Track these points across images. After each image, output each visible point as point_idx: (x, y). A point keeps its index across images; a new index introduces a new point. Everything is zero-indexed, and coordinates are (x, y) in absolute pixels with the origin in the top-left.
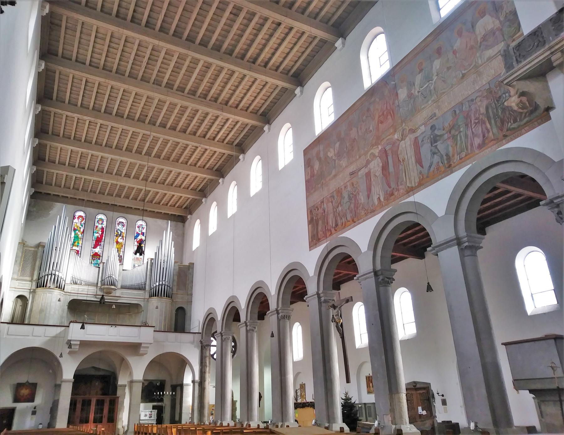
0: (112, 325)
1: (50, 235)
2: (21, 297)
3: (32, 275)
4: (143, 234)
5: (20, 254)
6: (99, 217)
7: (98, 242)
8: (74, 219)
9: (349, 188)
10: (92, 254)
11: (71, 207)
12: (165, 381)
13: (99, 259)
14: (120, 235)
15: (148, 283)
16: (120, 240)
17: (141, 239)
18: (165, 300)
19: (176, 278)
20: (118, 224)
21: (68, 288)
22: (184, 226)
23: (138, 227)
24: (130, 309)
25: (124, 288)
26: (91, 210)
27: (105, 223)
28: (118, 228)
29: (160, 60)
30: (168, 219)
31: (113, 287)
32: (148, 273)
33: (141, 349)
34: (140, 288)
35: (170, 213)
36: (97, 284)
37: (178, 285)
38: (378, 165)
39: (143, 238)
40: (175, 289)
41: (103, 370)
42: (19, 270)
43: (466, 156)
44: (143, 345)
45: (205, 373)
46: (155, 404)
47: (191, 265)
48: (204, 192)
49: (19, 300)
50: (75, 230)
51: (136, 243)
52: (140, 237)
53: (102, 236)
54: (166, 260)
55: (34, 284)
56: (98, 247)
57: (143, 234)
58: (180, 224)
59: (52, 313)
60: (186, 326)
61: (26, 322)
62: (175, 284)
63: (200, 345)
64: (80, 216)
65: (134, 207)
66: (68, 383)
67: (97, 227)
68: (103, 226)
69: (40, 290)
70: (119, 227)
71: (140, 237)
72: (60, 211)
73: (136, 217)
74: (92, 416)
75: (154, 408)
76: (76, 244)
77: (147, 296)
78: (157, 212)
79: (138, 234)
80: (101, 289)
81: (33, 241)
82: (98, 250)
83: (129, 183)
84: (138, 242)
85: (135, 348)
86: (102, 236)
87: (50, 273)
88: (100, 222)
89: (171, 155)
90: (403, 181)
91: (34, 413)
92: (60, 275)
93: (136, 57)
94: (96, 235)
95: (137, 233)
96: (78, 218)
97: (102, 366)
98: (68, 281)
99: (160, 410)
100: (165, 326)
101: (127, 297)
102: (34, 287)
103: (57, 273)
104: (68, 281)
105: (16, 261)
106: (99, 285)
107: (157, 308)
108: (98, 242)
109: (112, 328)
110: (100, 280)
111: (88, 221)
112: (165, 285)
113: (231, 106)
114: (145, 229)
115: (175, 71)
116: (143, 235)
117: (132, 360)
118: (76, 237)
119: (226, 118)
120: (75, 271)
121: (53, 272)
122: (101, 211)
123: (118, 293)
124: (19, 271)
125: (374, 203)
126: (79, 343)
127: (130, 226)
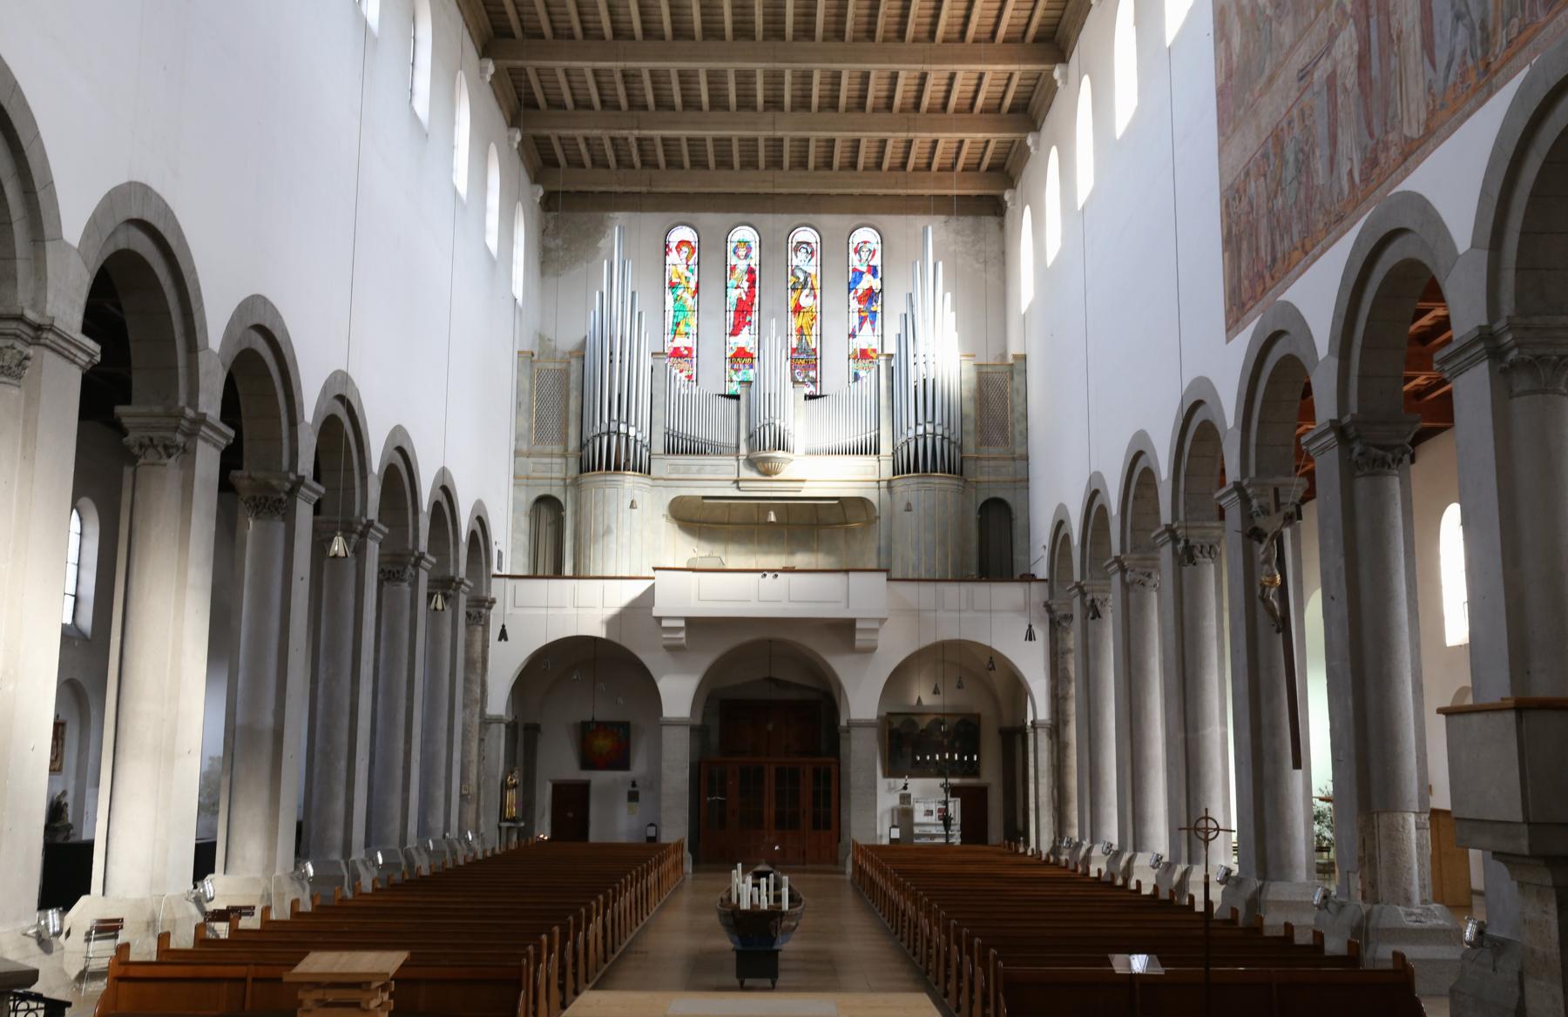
1: (593, 318)
3: (564, 440)
4: (873, 271)
5: (526, 384)
7: (743, 309)
8: (666, 254)
9: (1297, 131)
10: (729, 354)
11: (651, 221)
12: (979, 716)
13: (751, 366)
14: (804, 287)
16: (806, 301)
17: (871, 289)
19: (970, 409)
20: (796, 250)
22: (1002, 226)
23: (857, 251)
26: (710, 219)
27: (755, 253)
33: (858, 636)
36: (738, 447)
38: (1351, 47)
39: (876, 284)
43: (1520, 33)
44: (859, 625)
45: (1065, 698)
46: (954, 781)
48: (1028, 111)
49: (544, 510)
51: (855, 305)
57: (873, 271)
58: (990, 222)
63: (1047, 616)
64: (682, 243)
67: (733, 268)
69: (588, 477)
70: (801, 261)
71: (863, 285)
73: (846, 220)
74: (769, 811)
75: (954, 791)
76: (682, 328)
81: (566, 340)
82: (745, 339)
85: (843, 630)
87: (604, 429)
89: (875, 23)
90: (1395, 116)
91: (633, 797)
92: (632, 432)
94: (734, 295)
95: (855, 270)
96: (678, 247)
97: (794, 677)
99: (974, 802)
102: (573, 470)
104: (658, 447)
105: (519, 405)
106: (743, 450)
107: (909, 508)
110: (743, 436)
111: (709, 252)
112: (934, 435)
114: (878, 254)
121: (613, 427)
122: (739, 217)
125: (1341, 192)
126: (682, 624)
127: (832, 250)
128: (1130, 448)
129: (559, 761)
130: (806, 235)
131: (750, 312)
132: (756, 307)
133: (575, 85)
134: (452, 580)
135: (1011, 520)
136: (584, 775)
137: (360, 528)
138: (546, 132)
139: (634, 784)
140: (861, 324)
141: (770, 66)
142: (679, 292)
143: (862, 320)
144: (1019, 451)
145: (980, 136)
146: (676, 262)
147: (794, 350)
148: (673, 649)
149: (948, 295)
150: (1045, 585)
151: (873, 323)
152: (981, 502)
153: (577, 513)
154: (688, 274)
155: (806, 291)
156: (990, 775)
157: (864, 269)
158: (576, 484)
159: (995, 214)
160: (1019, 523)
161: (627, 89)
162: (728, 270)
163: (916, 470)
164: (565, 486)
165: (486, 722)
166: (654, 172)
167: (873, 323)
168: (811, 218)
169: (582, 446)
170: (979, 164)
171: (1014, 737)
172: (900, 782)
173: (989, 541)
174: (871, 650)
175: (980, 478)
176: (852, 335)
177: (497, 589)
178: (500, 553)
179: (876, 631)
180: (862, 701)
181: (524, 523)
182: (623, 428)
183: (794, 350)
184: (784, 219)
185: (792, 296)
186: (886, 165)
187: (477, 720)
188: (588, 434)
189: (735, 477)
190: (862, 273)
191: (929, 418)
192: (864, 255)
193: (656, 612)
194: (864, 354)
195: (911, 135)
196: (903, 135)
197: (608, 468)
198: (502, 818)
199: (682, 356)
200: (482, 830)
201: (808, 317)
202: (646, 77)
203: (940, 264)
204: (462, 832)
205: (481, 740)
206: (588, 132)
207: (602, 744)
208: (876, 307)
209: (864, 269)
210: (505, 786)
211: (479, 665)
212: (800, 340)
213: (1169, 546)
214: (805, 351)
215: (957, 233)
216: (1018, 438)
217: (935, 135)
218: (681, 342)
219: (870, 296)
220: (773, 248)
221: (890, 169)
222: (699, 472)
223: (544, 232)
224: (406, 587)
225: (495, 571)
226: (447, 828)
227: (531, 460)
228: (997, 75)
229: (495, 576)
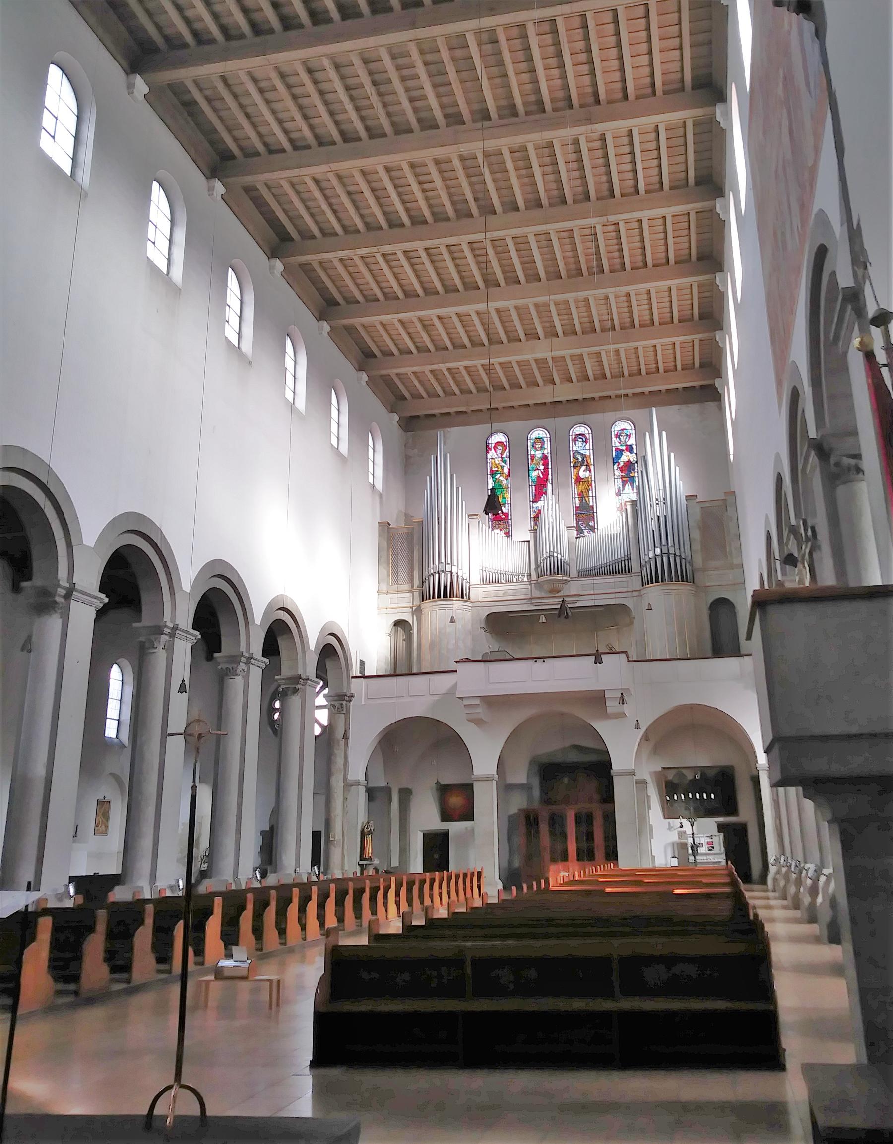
0: (535, 659)
2: (398, 623)
4: (630, 449)
6: (533, 437)
8: (487, 452)
11: (476, 431)
15: (633, 556)
16: (583, 473)
17: (629, 461)
18: (681, 589)
19: (696, 534)
20: (575, 440)
21: (478, 593)
23: (617, 436)
24: (613, 615)
27: (547, 445)
28: (575, 449)
29: (394, 75)
30: (649, 405)
31: (559, 577)
34: (621, 568)
39: (632, 457)
42: (388, 572)
50: (493, 473)
51: (618, 473)
52: (625, 457)
53: (545, 473)
55: (417, 594)
57: (630, 449)
59: (451, 646)
62: (697, 546)
64: (498, 443)
65: (596, 395)
67: (533, 457)
68: (546, 452)
69: (427, 605)
71: (625, 457)
72: (448, 442)
77: (636, 583)
78: (634, 394)
79: (620, 452)
80: (539, 585)
83: (542, 350)
84: (621, 469)
86: (545, 473)
88: (538, 446)
92: (454, 570)
93: (353, 92)
94: (534, 474)
95: (617, 449)
96: (495, 448)
98: (475, 579)
102: (417, 602)
103: (448, 568)
104: (475, 579)
105: (380, 558)
109: (536, 664)
110: (533, 566)
113: (610, 102)
114: (633, 436)
115: (440, 84)
116: (631, 451)
117: (602, 727)
119: (624, 132)
120: (486, 559)
123: (573, 588)
124: (388, 575)
127: (601, 437)
133: (394, 337)
134: (300, 677)
140: (624, 486)
143: (624, 483)
144: (736, 561)
148: (478, 722)
149: (672, 454)
154: (503, 464)
155: (584, 468)
157: (624, 448)
161: (430, 336)
184: (561, 421)
188: (426, 574)
189: (529, 596)
191: (664, 543)
197: (439, 596)
202: (515, 365)
206: (415, 369)
209: (624, 448)
212: (581, 501)
219: (629, 466)
220: (559, 441)
225: (356, 671)
228: (676, 290)
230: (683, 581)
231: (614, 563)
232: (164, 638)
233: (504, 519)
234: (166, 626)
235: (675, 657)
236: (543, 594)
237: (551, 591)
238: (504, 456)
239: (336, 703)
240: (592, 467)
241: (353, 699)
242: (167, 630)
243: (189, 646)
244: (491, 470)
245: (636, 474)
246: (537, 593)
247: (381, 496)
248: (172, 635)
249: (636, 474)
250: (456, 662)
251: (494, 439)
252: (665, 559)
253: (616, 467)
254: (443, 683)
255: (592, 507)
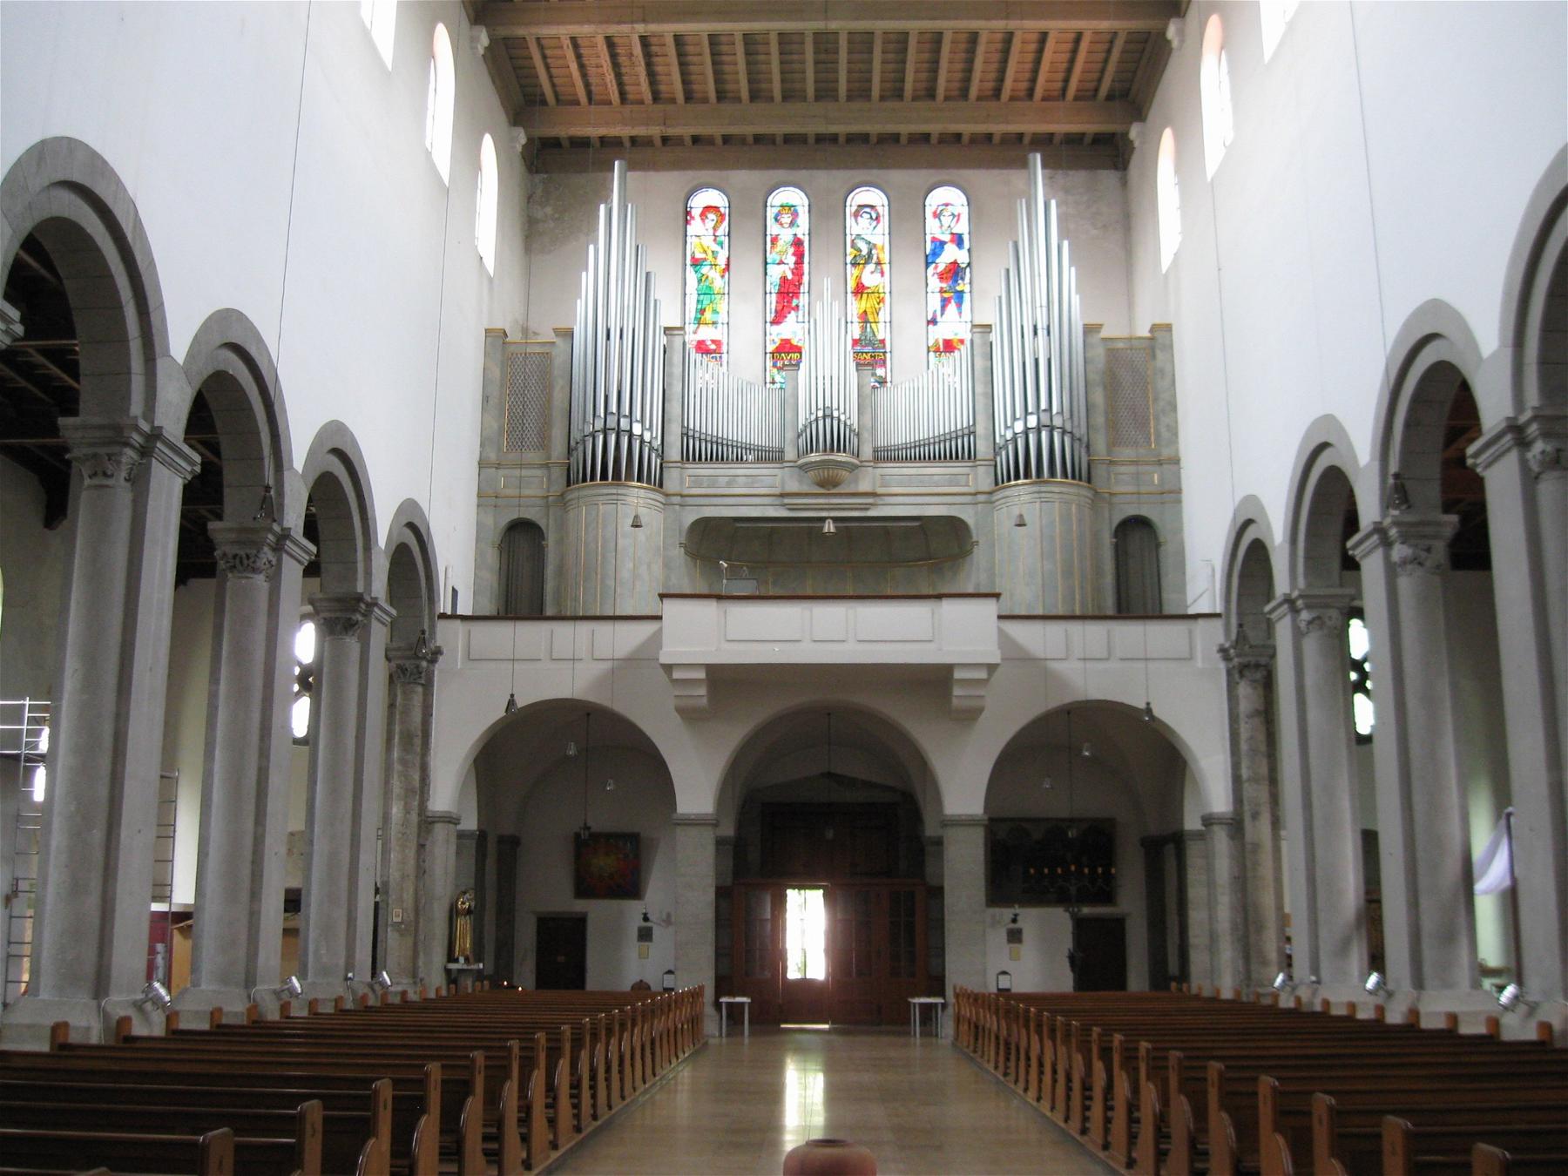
3: (544, 443)
4: (958, 240)
7: (788, 291)
8: (687, 222)
10: (771, 348)
11: (667, 182)
12: (1111, 822)
14: (867, 263)
15: (980, 430)
16: (870, 278)
17: (955, 263)
18: (1063, 492)
19: (1099, 397)
20: (856, 215)
22: (1124, 183)
23: (936, 215)
25: (888, 459)
26: (743, 178)
28: (855, 232)
31: (841, 457)
32: (979, 389)
34: (953, 450)
35: (1061, 127)
37: (1113, 425)
39: (962, 257)
40: (1100, 445)
41: (868, 785)
44: (958, 675)
47: (1162, 332)
51: (935, 284)
52: (951, 253)
54: (1041, 326)
55: (558, 474)
56: (792, 317)
57: (958, 240)
58: (1108, 178)
60: (1165, 595)
61: (549, 612)
62: (1099, 420)
64: (708, 209)
66: (693, 832)
67: (775, 240)
76: (708, 316)
77: (982, 479)
79: (939, 245)
84: (942, 277)
85: (932, 683)
87: (599, 425)
88: (786, 219)
94: (775, 273)
95: (934, 240)
96: (703, 215)
100: (1083, 604)
101: (907, 494)
104: (674, 453)
105: (486, 399)
108: (788, 291)
110: (790, 435)
112: (1052, 429)
118: (706, 292)
121: (612, 422)
126: (702, 675)
127: (907, 215)
128: (1407, 326)
129: (549, 887)
130: (871, 196)
131: (796, 294)
132: (804, 288)
134: (359, 598)
135: (1158, 545)
136: (580, 906)
137: (137, 438)
138: (521, 32)
139: (646, 919)
140: (943, 308)
141: (819, 25)
142: (705, 270)
143: (945, 303)
144: (1166, 453)
145: (1105, 25)
146: (701, 233)
147: (855, 342)
149: (1066, 244)
150: (1218, 625)
151: (959, 305)
152: (1116, 522)
153: (560, 542)
154: (716, 248)
155: (871, 267)
156: (1130, 903)
157: (947, 238)
158: (562, 501)
159: (1116, 168)
160: (1167, 550)
162: (765, 241)
163: (1027, 476)
164: (548, 507)
165: (427, 822)
166: (670, 107)
167: (959, 305)
168: (875, 174)
169: (570, 451)
170: (1096, 90)
171: (1167, 850)
172: (1007, 913)
173: (1129, 569)
174: (970, 715)
175: (1116, 489)
176: (933, 322)
177: (449, 636)
178: (455, 592)
179: (986, 681)
180: (962, 786)
181: (492, 557)
182: (624, 423)
183: (855, 342)
185: (852, 273)
186: (973, 92)
187: (414, 817)
188: (576, 435)
189: (777, 491)
190: (943, 243)
191: (1043, 405)
192: (946, 220)
193: (664, 659)
194: (949, 346)
195: (1012, 24)
196: (1000, 24)
197: (604, 476)
198: (451, 958)
199: (707, 352)
200: (421, 975)
201: (873, 301)
203: (1053, 203)
204: (375, 972)
205: (421, 846)
207: (604, 863)
208: (963, 286)
209: (947, 238)
210: (453, 913)
211: (418, 741)
212: (864, 329)
213: (1513, 457)
214: (871, 343)
215: (1067, 191)
216: (1165, 434)
217: (1042, 25)
218: (707, 334)
219: (954, 272)
220: (828, 213)
221: (979, 98)
222: (729, 485)
223: (529, 198)
224: (260, 581)
225: (444, 606)
226: (349, 966)
227: (501, 472)
229: (443, 616)
230: (1073, 477)
231: (943, 439)
232: (129, 455)
233: (714, 351)
234: (137, 428)
235: (1054, 613)
236: (805, 489)
237: (821, 484)
238: (720, 232)
239: (408, 664)
240: (886, 268)
241: (441, 658)
242: (137, 438)
243: (178, 485)
244: (693, 258)
245: (967, 289)
246: (793, 486)
247: (491, 280)
248: (146, 452)
249: (967, 289)
250: (662, 596)
251: (700, 201)
252: (1044, 435)
253: (931, 269)
254: (628, 638)
255: (883, 341)
